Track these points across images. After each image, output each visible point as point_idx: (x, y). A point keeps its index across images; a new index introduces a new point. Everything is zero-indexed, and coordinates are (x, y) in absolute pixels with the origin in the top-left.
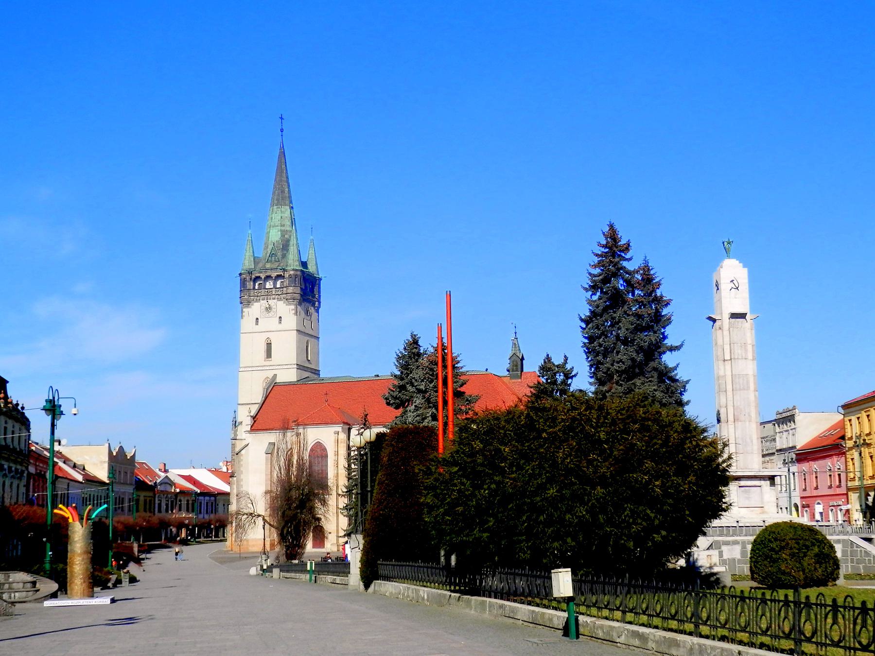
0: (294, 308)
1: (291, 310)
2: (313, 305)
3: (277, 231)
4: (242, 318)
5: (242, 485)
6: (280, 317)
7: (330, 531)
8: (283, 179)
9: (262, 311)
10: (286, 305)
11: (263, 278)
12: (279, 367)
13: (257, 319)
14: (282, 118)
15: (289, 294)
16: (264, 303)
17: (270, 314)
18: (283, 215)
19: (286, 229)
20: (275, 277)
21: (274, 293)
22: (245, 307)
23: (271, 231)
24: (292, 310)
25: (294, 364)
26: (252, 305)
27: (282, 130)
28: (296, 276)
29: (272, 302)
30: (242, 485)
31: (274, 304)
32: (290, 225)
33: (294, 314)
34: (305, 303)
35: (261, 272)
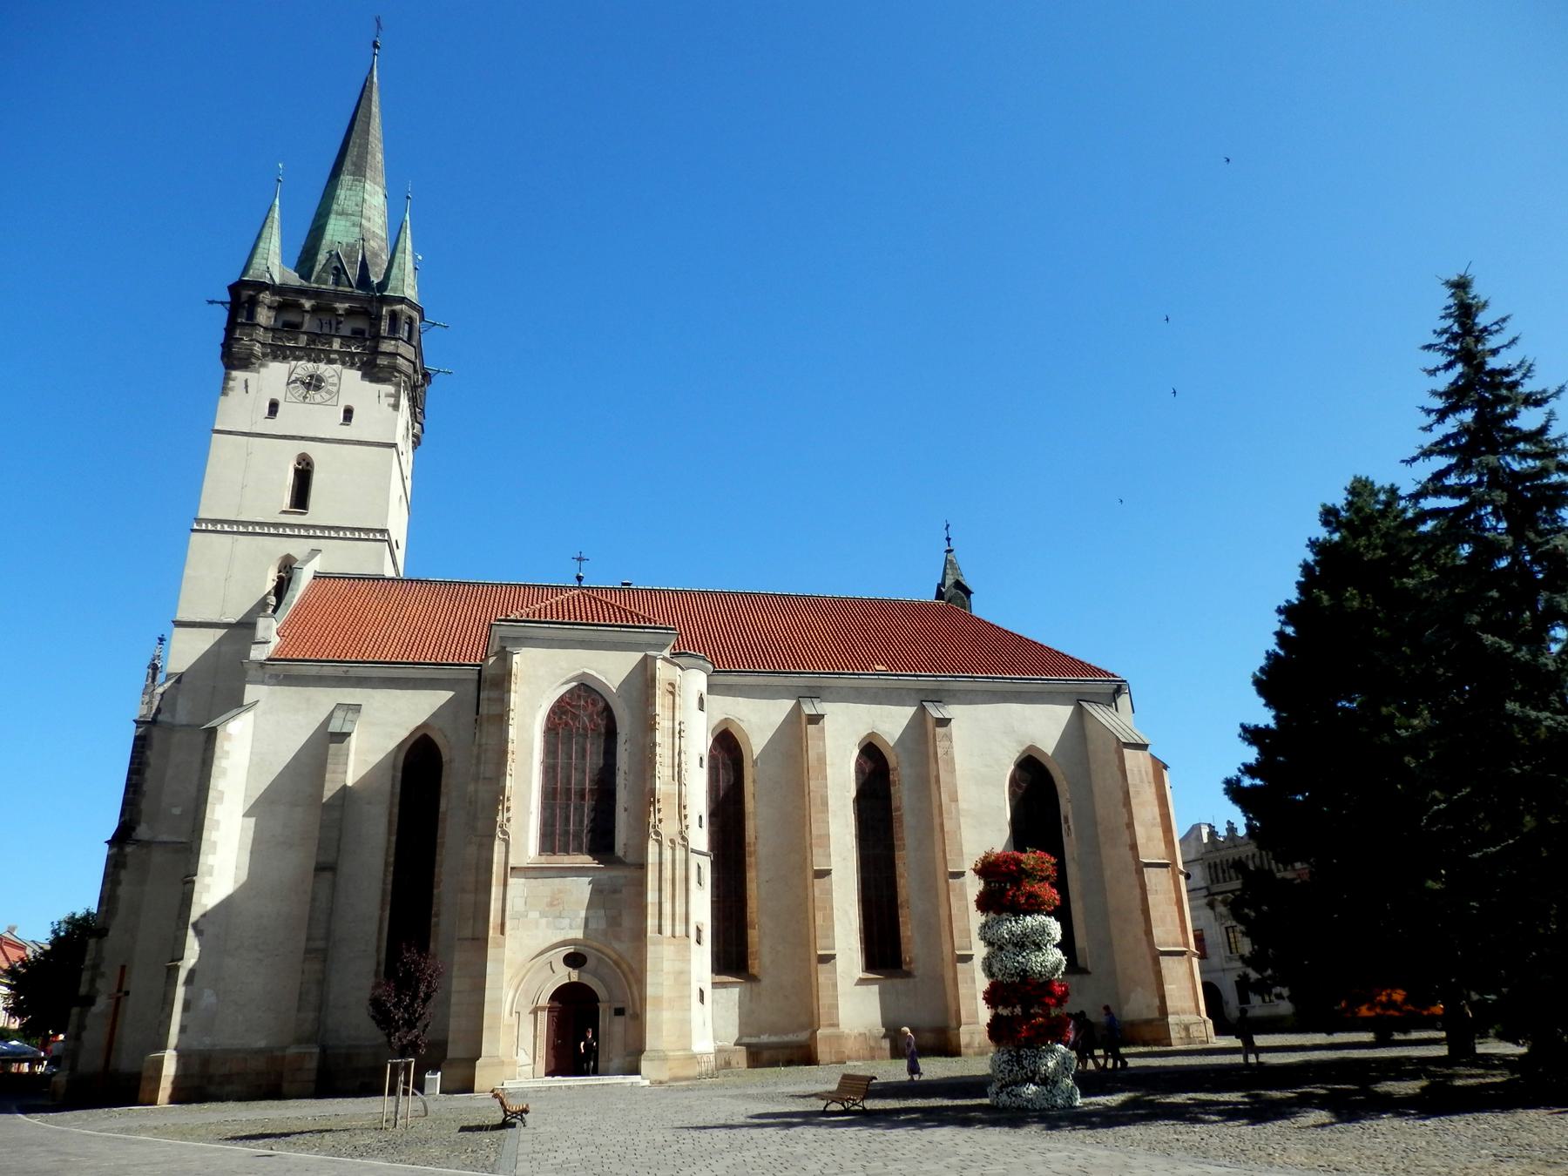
0: (393, 392)
1: (382, 395)
4: (225, 390)
5: (215, 843)
6: (348, 414)
7: (619, 1005)
13: (274, 407)
19: (372, 229)
20: (346, 310)
21: (336, 346)
24: (388, 395)
29: (323, 369)
30: (215, 843)
31: (333, 373)
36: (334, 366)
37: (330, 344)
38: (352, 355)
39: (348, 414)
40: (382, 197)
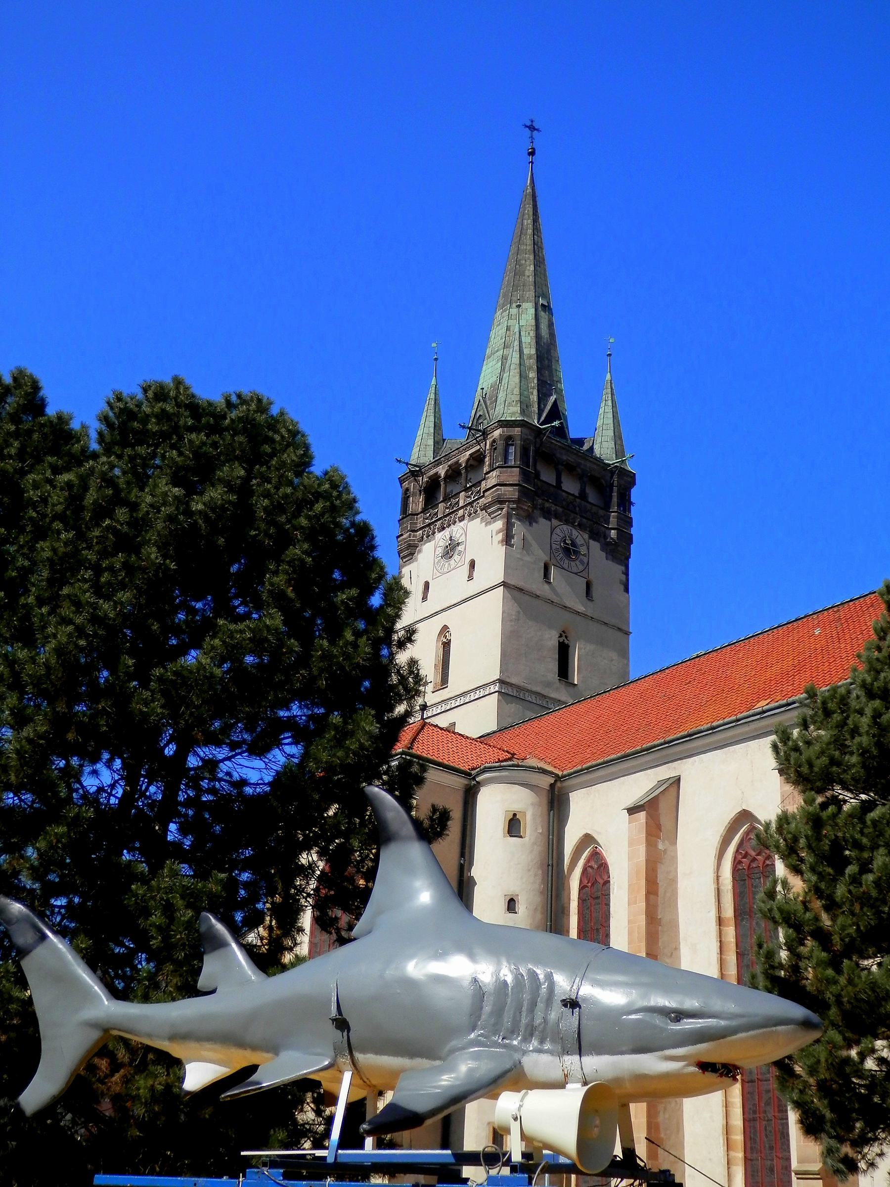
2: (597, 534)
3: (494, 362)
6: (472, 564)
8: (522, 247)
9: (436, 560)
10: (486, 525)
11: (442, 476)
12: (462, 700)
13: (427, 585)
14: (532, 128)
15: (487, 494)
16: (441, 538)
17: (452, 562)
18: (511, 322)
20: (468, 460)
21: (461, 504)
22: (406, 563)
23: (484, 368)
25: (493, 682)
26: (420, 551)
27: (532, 153)
28: (508, 440)
29: (456, 530)
31: (461, 531)
32: (530, 344)
33: (502, 541)
34: (555, 522)
35: (437, 463)
36: (462, 524)
37: (458, 503)
38: (471, 504)
39: (472, 564)
40: (532, 311)
